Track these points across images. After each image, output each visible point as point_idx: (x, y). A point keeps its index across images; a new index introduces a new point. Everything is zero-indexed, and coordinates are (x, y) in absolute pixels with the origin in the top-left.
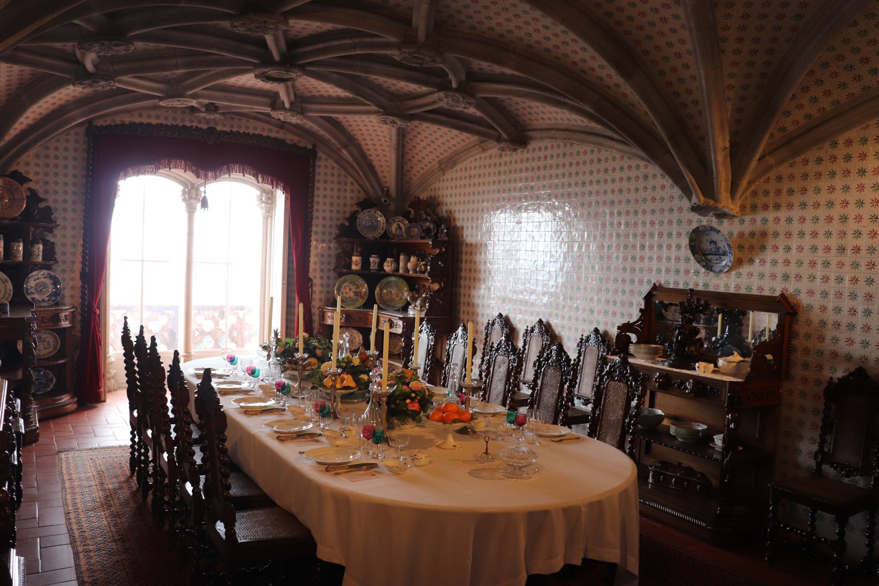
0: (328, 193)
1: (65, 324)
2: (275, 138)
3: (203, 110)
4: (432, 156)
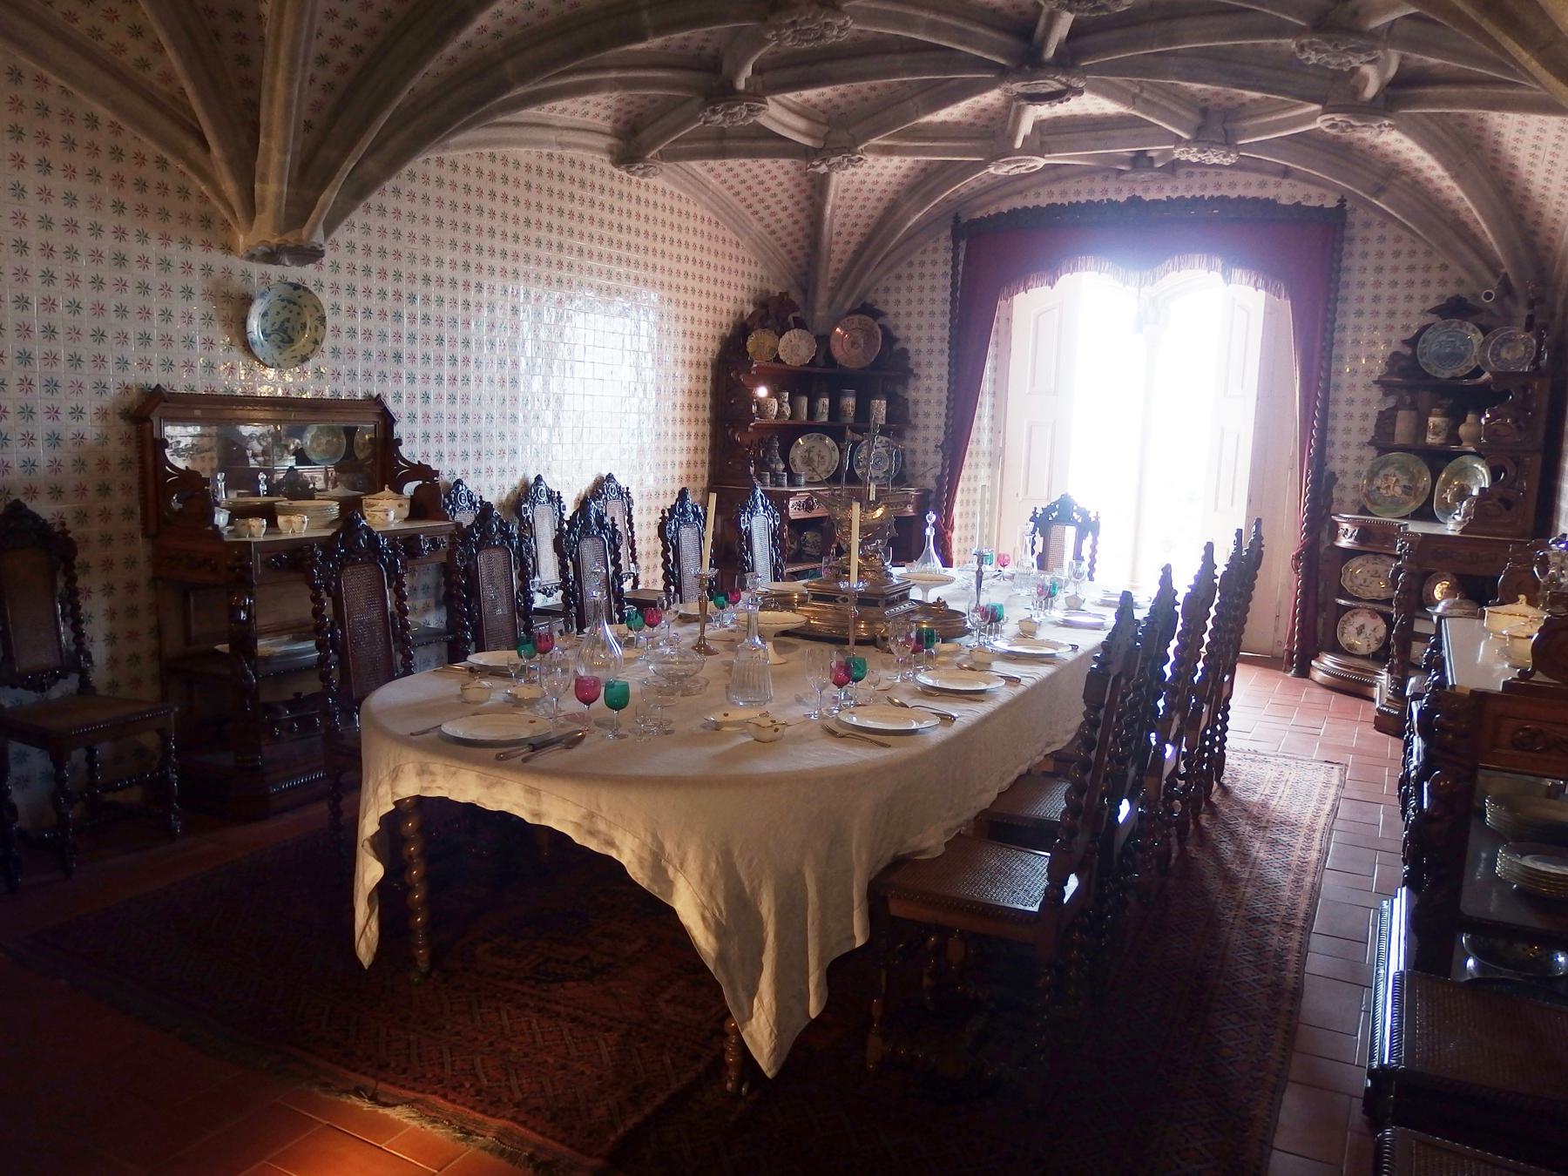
2: (1255, 200)
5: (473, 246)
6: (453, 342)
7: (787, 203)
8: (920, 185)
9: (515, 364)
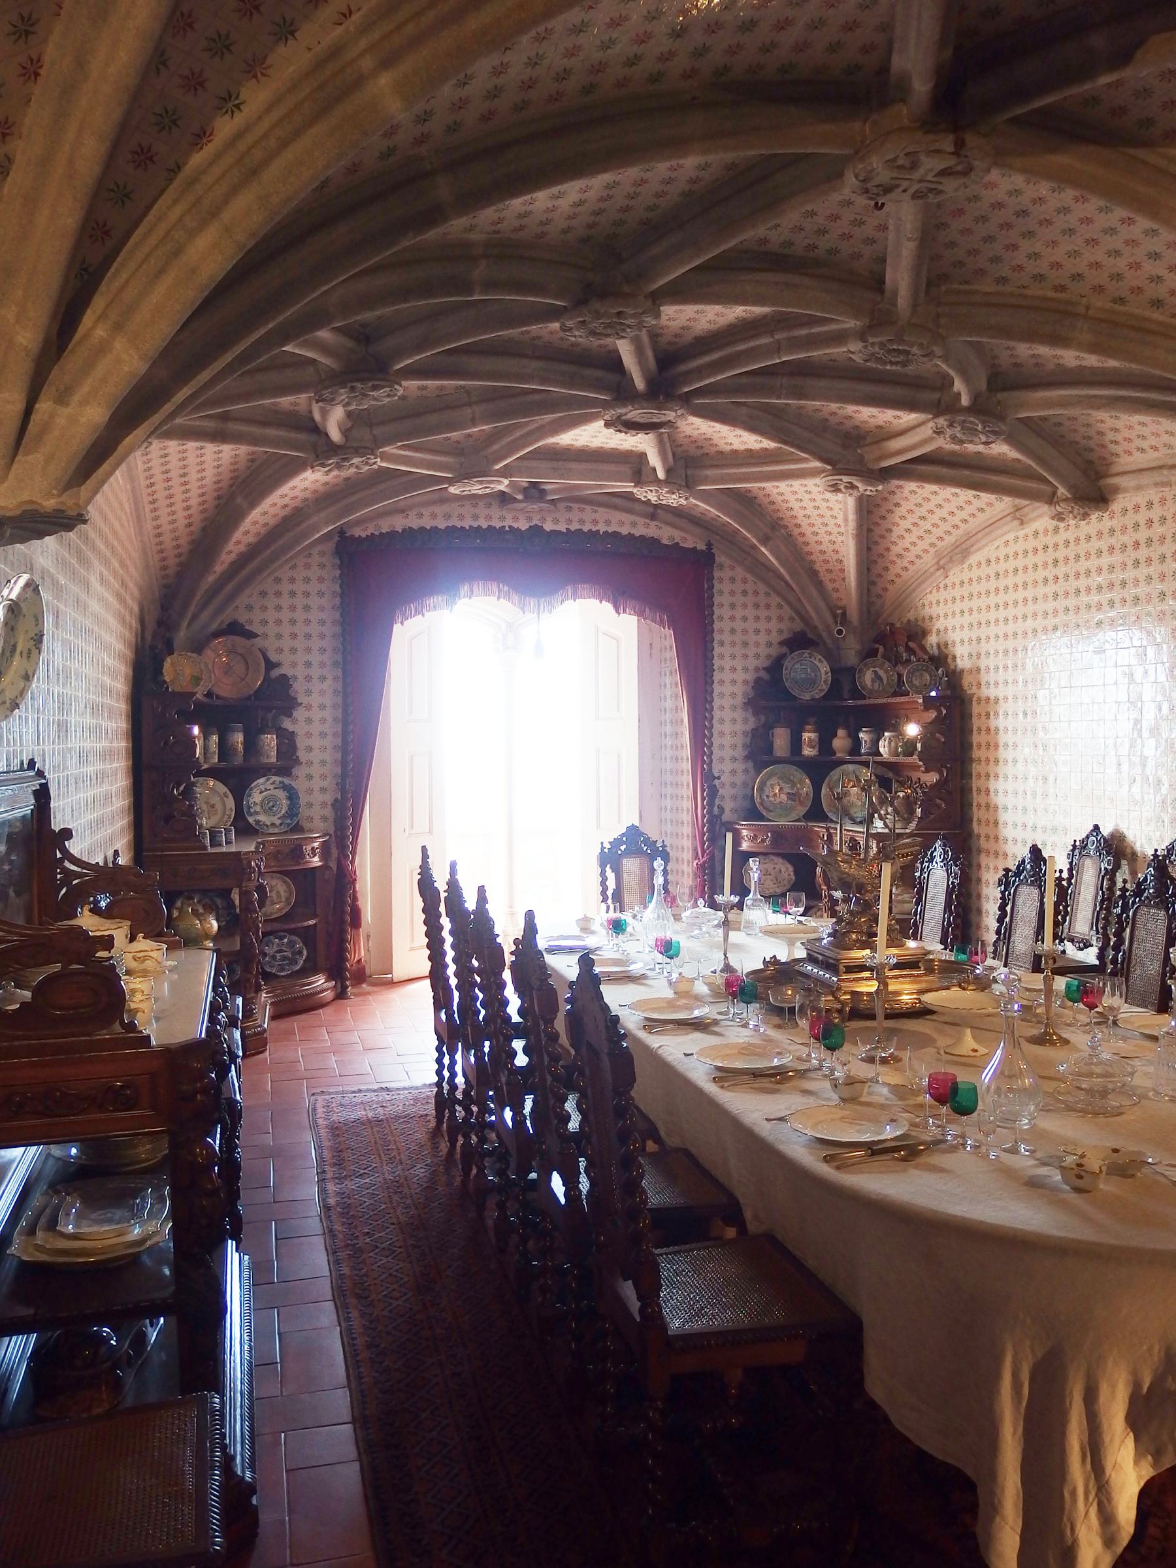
0: (739, 625)
1: (316, 861)
4: (922, 545)
7: (194, 502)
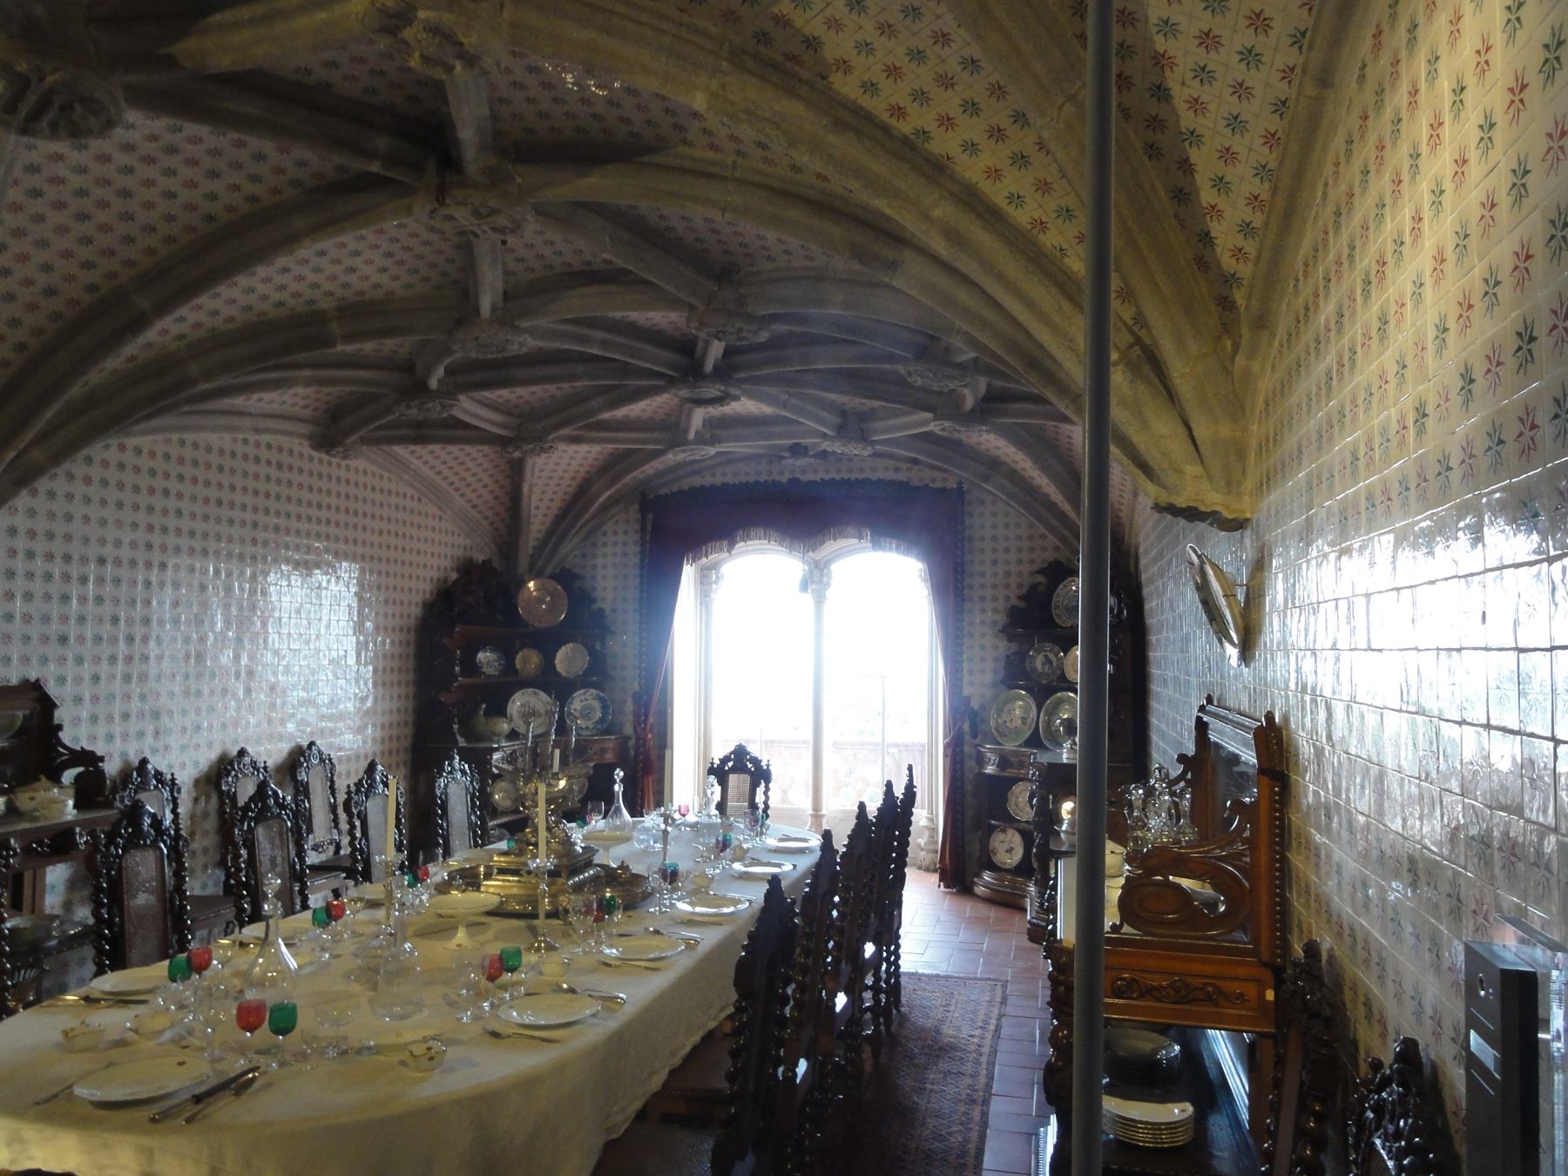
2: (892, 483)
3: (787, 455)
5: (157, 527)
6: (130, 621)
7: (488, 481)
8: (612, 468)
9: (202, 640)
